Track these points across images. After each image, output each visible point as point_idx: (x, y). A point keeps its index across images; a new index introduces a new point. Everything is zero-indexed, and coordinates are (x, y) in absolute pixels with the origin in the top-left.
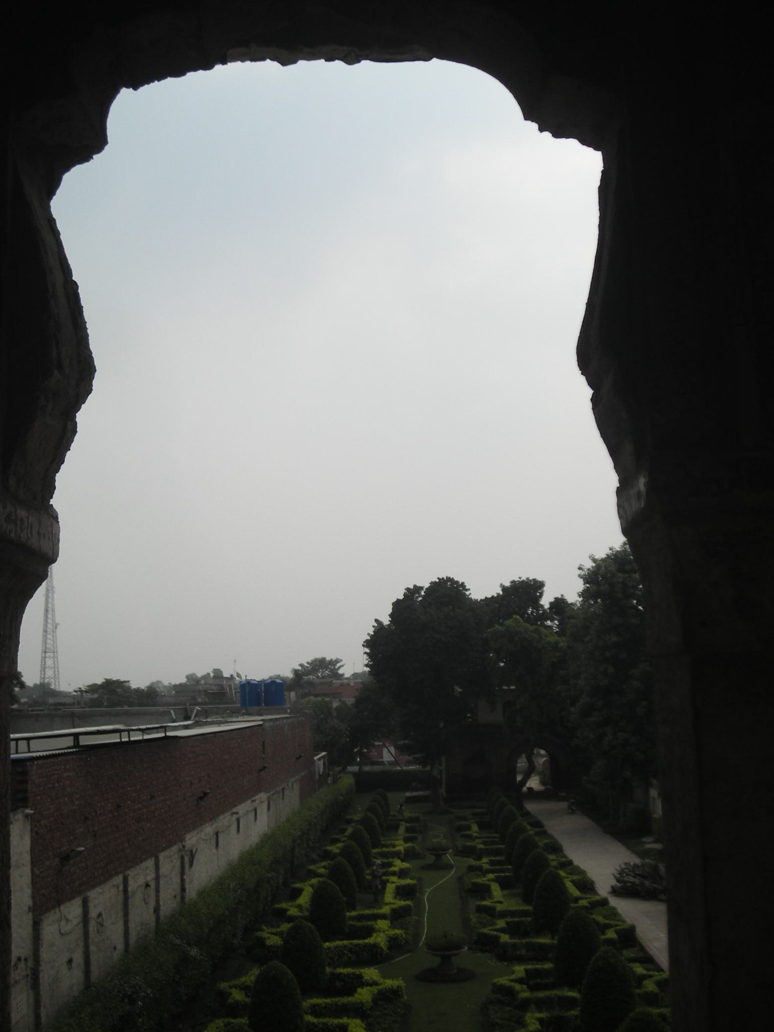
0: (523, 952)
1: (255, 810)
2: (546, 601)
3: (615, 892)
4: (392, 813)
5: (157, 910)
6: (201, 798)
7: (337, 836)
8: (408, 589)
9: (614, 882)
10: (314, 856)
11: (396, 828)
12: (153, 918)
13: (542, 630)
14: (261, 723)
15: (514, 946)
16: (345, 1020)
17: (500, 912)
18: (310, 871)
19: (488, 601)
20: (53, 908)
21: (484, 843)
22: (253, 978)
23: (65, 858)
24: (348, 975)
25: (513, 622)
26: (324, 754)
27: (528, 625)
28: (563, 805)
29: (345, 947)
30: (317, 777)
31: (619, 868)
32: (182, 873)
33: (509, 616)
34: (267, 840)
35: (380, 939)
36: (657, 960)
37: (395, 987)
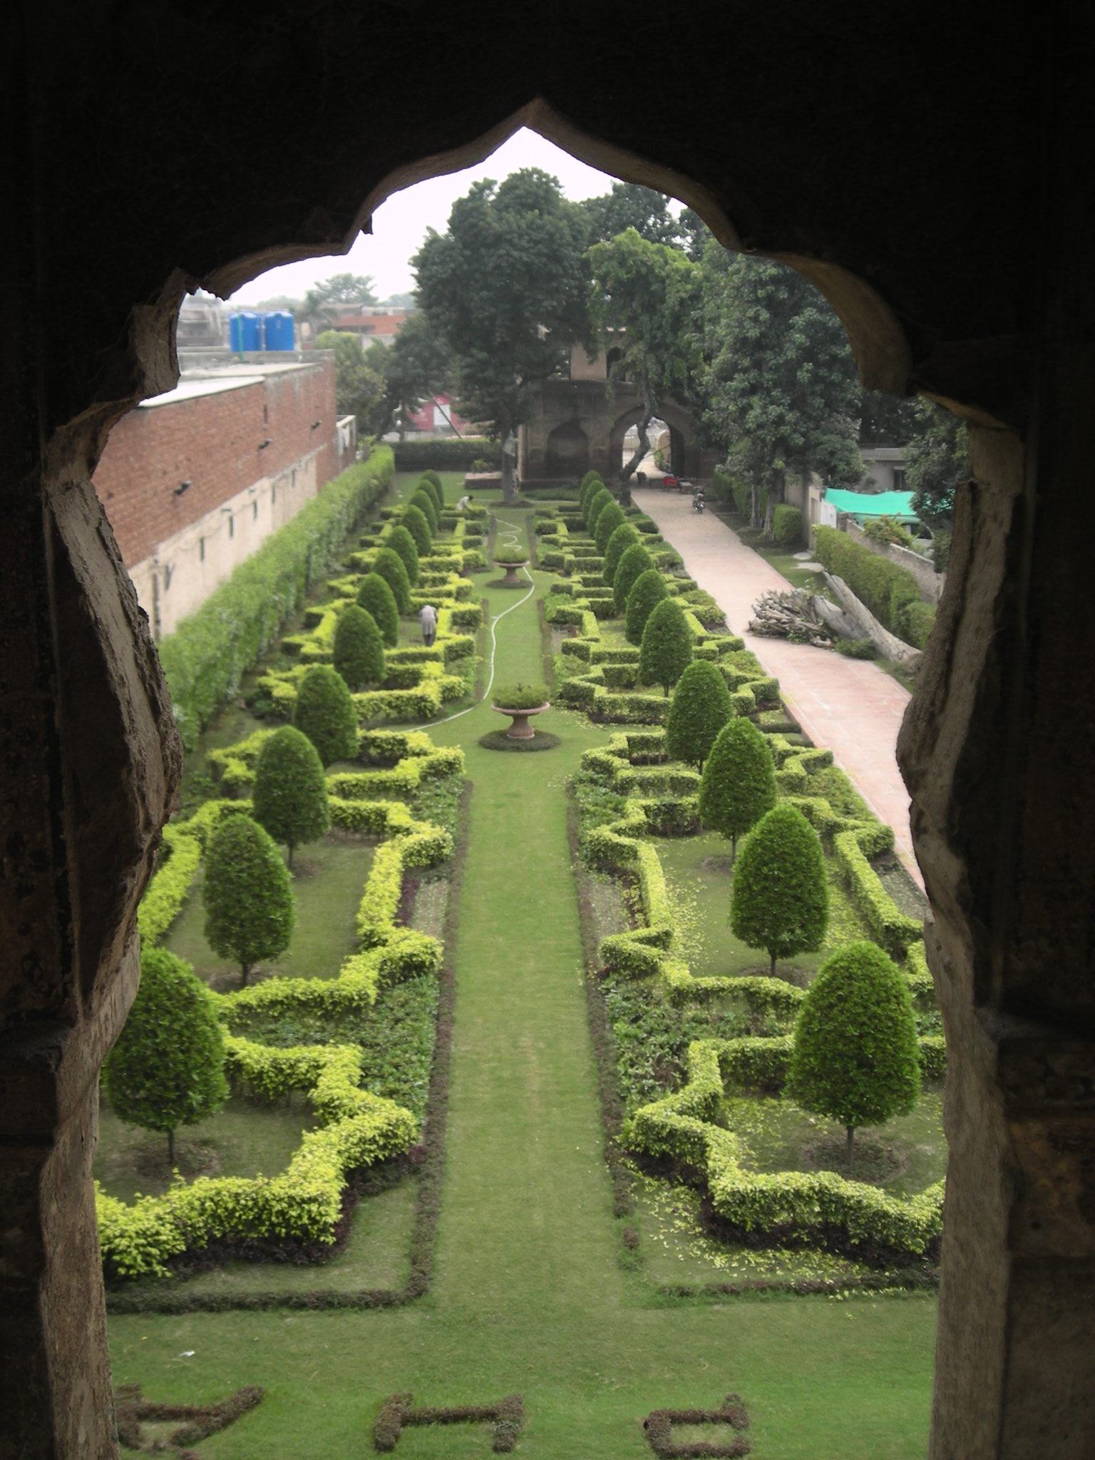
0: (625, 712)
1: (255, 504)
3: (752, 630)
4: (446, 505)
6: (179, 493)
7: (369, 538)
8: (476, 184)
10: (338, 566)
11: (452, 527)
13: (668, 250)
14: (261, 379)
15: (614, 704)
16: (383, 804)
18: (332, 589)
19: (592, 205)
21: (576, 553)
22: (257, 744)
24: (387, 741)
25: (629, 237)
26: (350, 418)
28: (688, 500)
29: (382, 699)
30: (341, 451)
31: (760, 598)
34: (274, 546)
35: (429, 690)
37: (451, 759)
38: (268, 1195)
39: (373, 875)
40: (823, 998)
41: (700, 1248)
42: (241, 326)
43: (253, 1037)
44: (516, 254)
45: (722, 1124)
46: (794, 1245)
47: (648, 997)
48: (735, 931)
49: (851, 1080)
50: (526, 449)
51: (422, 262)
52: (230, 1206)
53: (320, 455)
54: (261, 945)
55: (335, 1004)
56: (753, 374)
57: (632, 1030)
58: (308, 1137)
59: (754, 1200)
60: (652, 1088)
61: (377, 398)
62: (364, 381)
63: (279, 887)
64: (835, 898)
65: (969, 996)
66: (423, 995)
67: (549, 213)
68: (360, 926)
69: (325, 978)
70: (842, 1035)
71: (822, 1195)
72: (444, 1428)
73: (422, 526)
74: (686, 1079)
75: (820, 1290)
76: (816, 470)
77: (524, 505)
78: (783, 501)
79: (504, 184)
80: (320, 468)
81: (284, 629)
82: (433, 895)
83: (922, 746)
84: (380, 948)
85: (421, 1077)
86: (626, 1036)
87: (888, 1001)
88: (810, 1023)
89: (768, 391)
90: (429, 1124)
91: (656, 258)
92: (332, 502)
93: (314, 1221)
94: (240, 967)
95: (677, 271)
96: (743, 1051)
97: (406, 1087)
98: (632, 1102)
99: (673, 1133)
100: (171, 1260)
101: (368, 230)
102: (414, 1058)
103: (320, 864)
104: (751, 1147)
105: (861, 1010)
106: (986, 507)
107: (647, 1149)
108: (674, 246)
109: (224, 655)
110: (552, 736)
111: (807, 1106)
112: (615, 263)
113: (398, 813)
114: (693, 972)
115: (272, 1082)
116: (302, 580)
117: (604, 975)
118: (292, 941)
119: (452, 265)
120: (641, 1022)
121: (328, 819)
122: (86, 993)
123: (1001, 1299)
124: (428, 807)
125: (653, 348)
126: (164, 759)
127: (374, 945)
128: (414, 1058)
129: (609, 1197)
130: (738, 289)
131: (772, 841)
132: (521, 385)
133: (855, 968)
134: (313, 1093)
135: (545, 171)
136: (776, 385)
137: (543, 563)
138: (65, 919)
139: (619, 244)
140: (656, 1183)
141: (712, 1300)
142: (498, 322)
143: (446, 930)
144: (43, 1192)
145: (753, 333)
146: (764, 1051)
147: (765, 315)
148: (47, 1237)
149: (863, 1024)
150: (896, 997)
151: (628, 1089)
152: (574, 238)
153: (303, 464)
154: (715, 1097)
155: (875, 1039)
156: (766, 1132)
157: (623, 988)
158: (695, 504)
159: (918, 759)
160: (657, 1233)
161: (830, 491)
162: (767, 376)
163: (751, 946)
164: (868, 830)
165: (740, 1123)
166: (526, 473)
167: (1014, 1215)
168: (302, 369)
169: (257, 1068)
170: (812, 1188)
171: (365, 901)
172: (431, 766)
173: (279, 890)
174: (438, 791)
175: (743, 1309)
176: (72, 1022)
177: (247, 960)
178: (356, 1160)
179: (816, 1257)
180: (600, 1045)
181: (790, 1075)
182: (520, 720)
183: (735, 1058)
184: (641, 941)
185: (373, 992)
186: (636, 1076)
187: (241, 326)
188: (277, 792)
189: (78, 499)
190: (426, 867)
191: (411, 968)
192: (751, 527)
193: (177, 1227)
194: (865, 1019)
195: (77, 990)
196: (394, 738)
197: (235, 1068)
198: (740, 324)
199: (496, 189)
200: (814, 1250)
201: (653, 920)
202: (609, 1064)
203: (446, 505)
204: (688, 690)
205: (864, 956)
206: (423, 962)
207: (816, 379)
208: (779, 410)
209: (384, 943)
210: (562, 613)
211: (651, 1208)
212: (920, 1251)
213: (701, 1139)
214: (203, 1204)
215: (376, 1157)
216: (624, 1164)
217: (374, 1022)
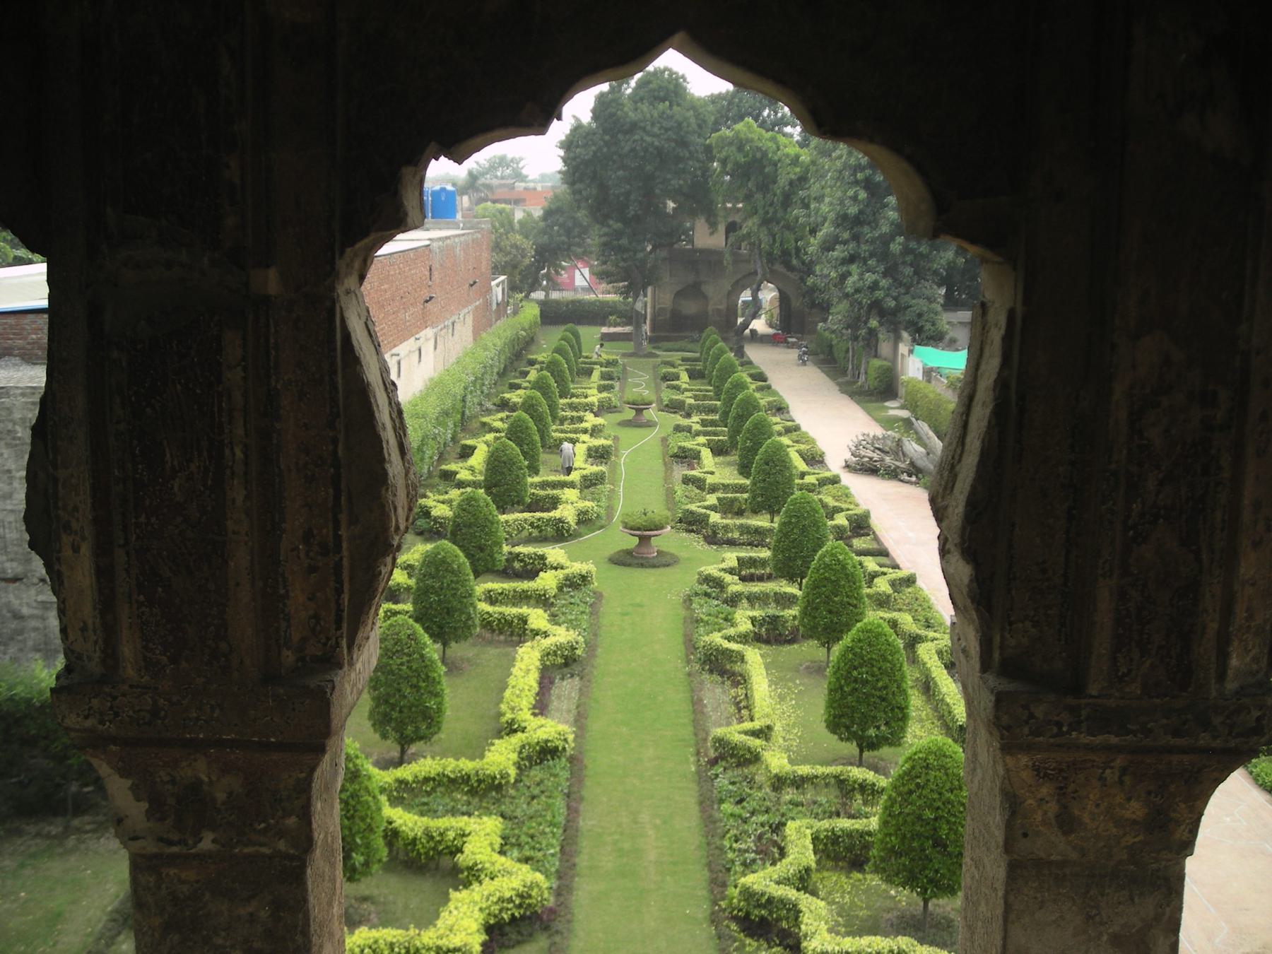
0: (736, 535)
3: (848, 467)
7: (516, 381)
9: (848, 456)
10: (489, 405)
11: (589, 373)
14: (428, 243)
16: (524, 610)
18: (484, 424)
19: (715, 99)
21: (696, 398)
22: (417, 556)
25: (746, 127)
26: (503, 278)
28: (793, 354)
33: (741, 118)
34: (434, 386)
35: (567, 512)
37: (584, 572)
38: (418, 944)
39: (514, 671)
40: (904, 785)
43: (408, 807)
45: (814, 893)
47: (751, 782)
48: (828, 727)
49: (927, 856)
50: (654, 307)
53: (477, 307)
54: (417, 728)
55: (479, 781)
56: (852, 245)
57: (737, 810)
58: (454, 895)
60: (754, 861)
61: (527, 261)
62: (515, 246)
64: (916, 701)
65: (978, 666)
66: (556, 776)
67: (678, 105)
68: (503, 715)
69: (472, 759)
70: (919, 818)
74: (783, 853)
76: (906, 329)
78: (876, 356)
81: (442, 458)
82: (566, 689)
83: (945, 488)
84: (519, 734)
85: (552, 846)
86: (732, 815)
88: (892, 806)
89: (865, 261)
90: (559, 887)
92: (486, 349)
94: (399, 749)
95: (787, 155)
97: (539, 855)
98: (736, 873)
99: (770, 900)
101: (559, 118)
102: (547, 830)
103: (468, 660)
104: (839, 915)
105: (936, 796)
106: (991, 317)
108: (785, 135)
110: (672, 555)
111: (888, 880)
112: (734, 148)
113: (537, 618)
114: (791, 762)
117: (713, 762)
118: (444, 726)
119: (593, 148)
120: (745, 804)
121: (477, 622)
122: (350, 647)
123: (1000, 894)
125: (765, 222)
126: (407, 486)
127: (515, 731)
128: (547, 830)
130: (840, 172)
133: (931, 759)
134: (460, 858)
135: (675, 69)
136: (872, 255)
138: (339, 591)
140: (755, 944)
142: (632, 197)
143: (576, 721)
144: (314, 790)
145: (853, 210)
146: (851, 832)
147: (863, 195)
148: (314, 826)
149: (938, 808)
151: (733, 861)
152: (700, 126)
154: (808, 870)
155: (948, 822)
156: (852, 902)
157: (730, 773)
158: (800, 358)
159: (943, 498)
161: (917, 347)
162: (864, 247)
163: (842, 739)
165: (830, 893)
166: (653, 329)
167: (1009, 826)
169: (411, 835)
171: (507, 693)
172: (567, 578)
173: (435, 682)
176: (340, 666)
177: (405, 742)
178: (495, 916)
180: (709, 823)
181: (874, 852)
182: (644, 540)
183: (826, 837)
184: (746, 733)
185: (513, 772)
186: (740, 850)
188: (433, 598)
189: (354, 301)
190: (562, 664)
191: (545, 753)
192: (849, 378)
194: (939, 804)
195: (344, 643)
197: (393, 835)
198: (842, 203)
201: (757, 716)
202: (716, 839)
204: (791, 517)
205: (939, 749)
206: (557, 748)
207: (907, 251)
208: (874, 277)
209: (523, 730)
210: (683, 449)
213: (795, 906)
215: (513, 915)
216: (728, 927)
217: (514, 798)
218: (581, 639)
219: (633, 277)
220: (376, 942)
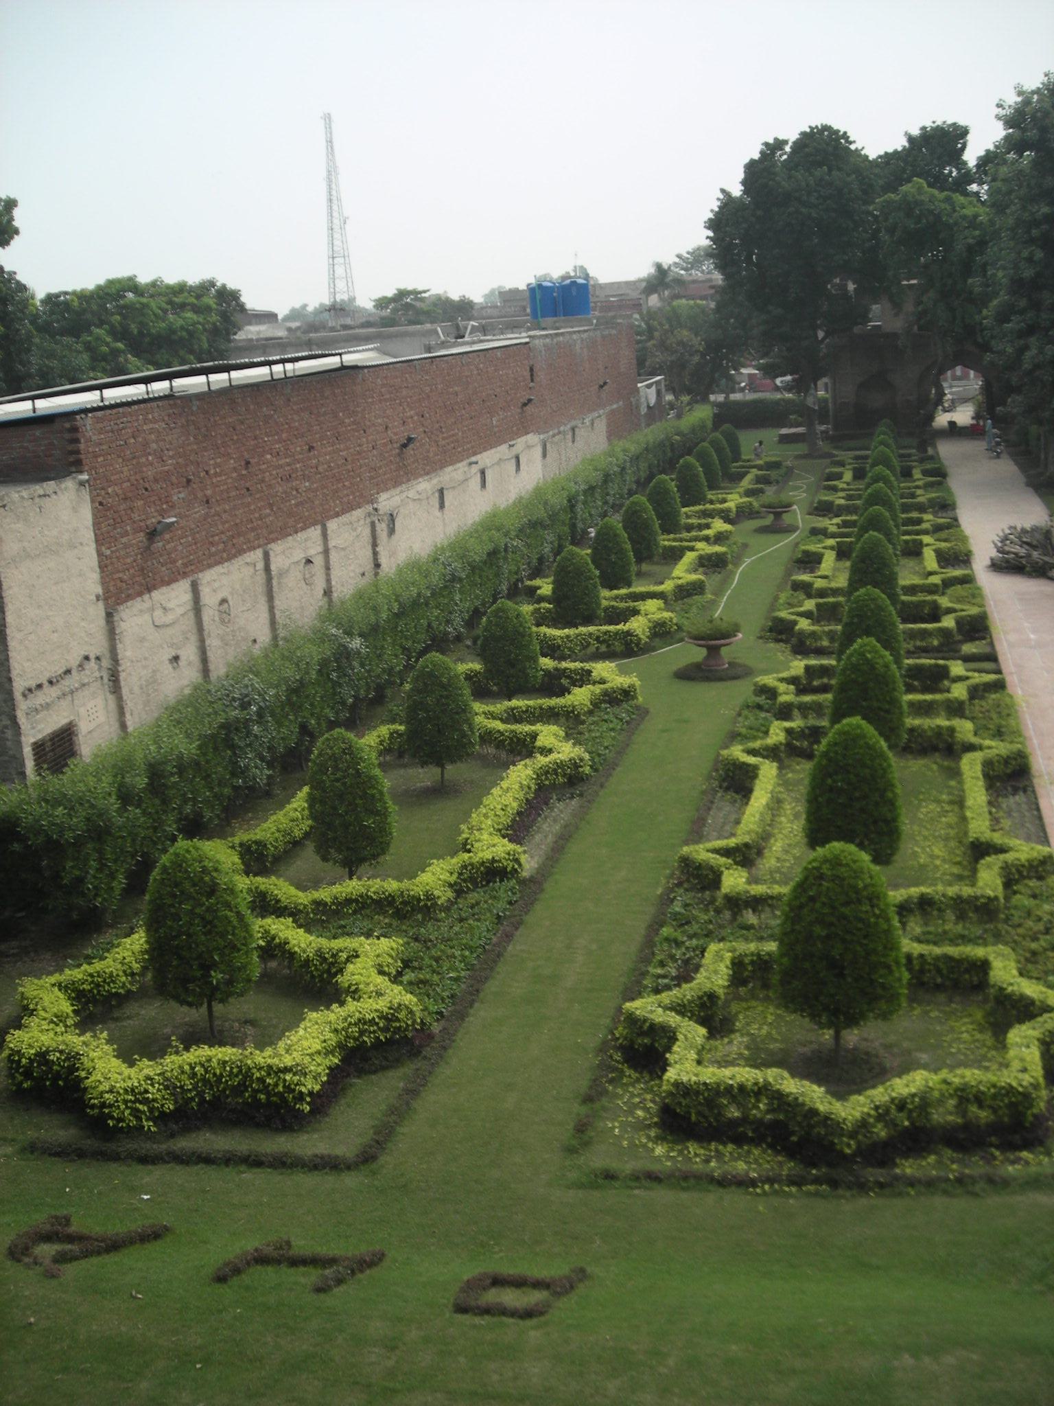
0: (825, 643)
1: (517, 458)
2: (971, 156)
4: (744, 457)
5: (328, 592)
6: (405, 446)
8: (766, 144)
9: (994, 553)
11: (737, 478)
12: (324, 602)
15: (813, 633)
17: (818, 590)
19: (888, 158)
20: (140, 594)
21: (849, 498)
23: (152, 534)
24: (575, 671)
25: (917, 187)
26: (659, 378)
27: (935, 192)
29: (591, 634)
30: (644, 410)
31: (1001, 534)
32: (374, 545)
33: (909, 180)
35: (638, 625)
36: (1001, 658)
38: (249, 1062)
41: (649, 1137)
42: (538, 297)
44: (803, 210)
46: (739, 1140)
51: (716, 224)
52: (218, 1072)
53: (612, 412)
55: (405, 903)
59: (698, 1093)
61: (696, 359)
62: (681, 343)
63: (373, 796)
67: (839, 169)
71: (762, 1090)
72: (292, 1270)
73: (697, 476)
75: (744, 1183)
77: (830, 455)
79: (794, 143)
80: (608, 425)
87: (859, 901)
91: (943, 206)
93: (288, 1089)
95: (964, 217)
96: (759, 955)
97: (436, 978)
100: (162, 1118)
102: (458, 953)
104: (747, 1048)
105: (826, 911)
107: (632, 1042)
108: (966, 194)
109: (433, 594)
113: (548, 734)
115: (316, 969)
116: (567, 529)
119: (744, 225)
124: (590, 731)
129: (584, 1084)
131: (836, 753)
132: (824, 339)
134: (339, 978)
137: (816, 509)
139: (905, 195)
141: (634, 1184)
145: (1028, 273)
147: (1039, 255)
149: (832, 924)
150: (870, 899)
153: (587, 421)
156: (769, 1034)
157: (690, 895)
160: (613, 1120)
164: (998, 748)
168: (585, 331)
170: (756, 1084)
172: (605, 693)
174: (606, 717)
175: (662, 1196)
178: (355, 1039)
179: (756, 1152)
183: (752, 962)
187: (538, 297)
193: (167, 1088)
194: (833, 919)
196: (582, 669)
199: (788, 149)
200: (757, 1145)
203: (744, 457)
210: (806, 553)
211: (617, 1096)
212: (848, 1151)
214: (192, 1068)
216: (611, 1057)
218: (587, 756)
219: (806, 370)
220: (209, 1060)
